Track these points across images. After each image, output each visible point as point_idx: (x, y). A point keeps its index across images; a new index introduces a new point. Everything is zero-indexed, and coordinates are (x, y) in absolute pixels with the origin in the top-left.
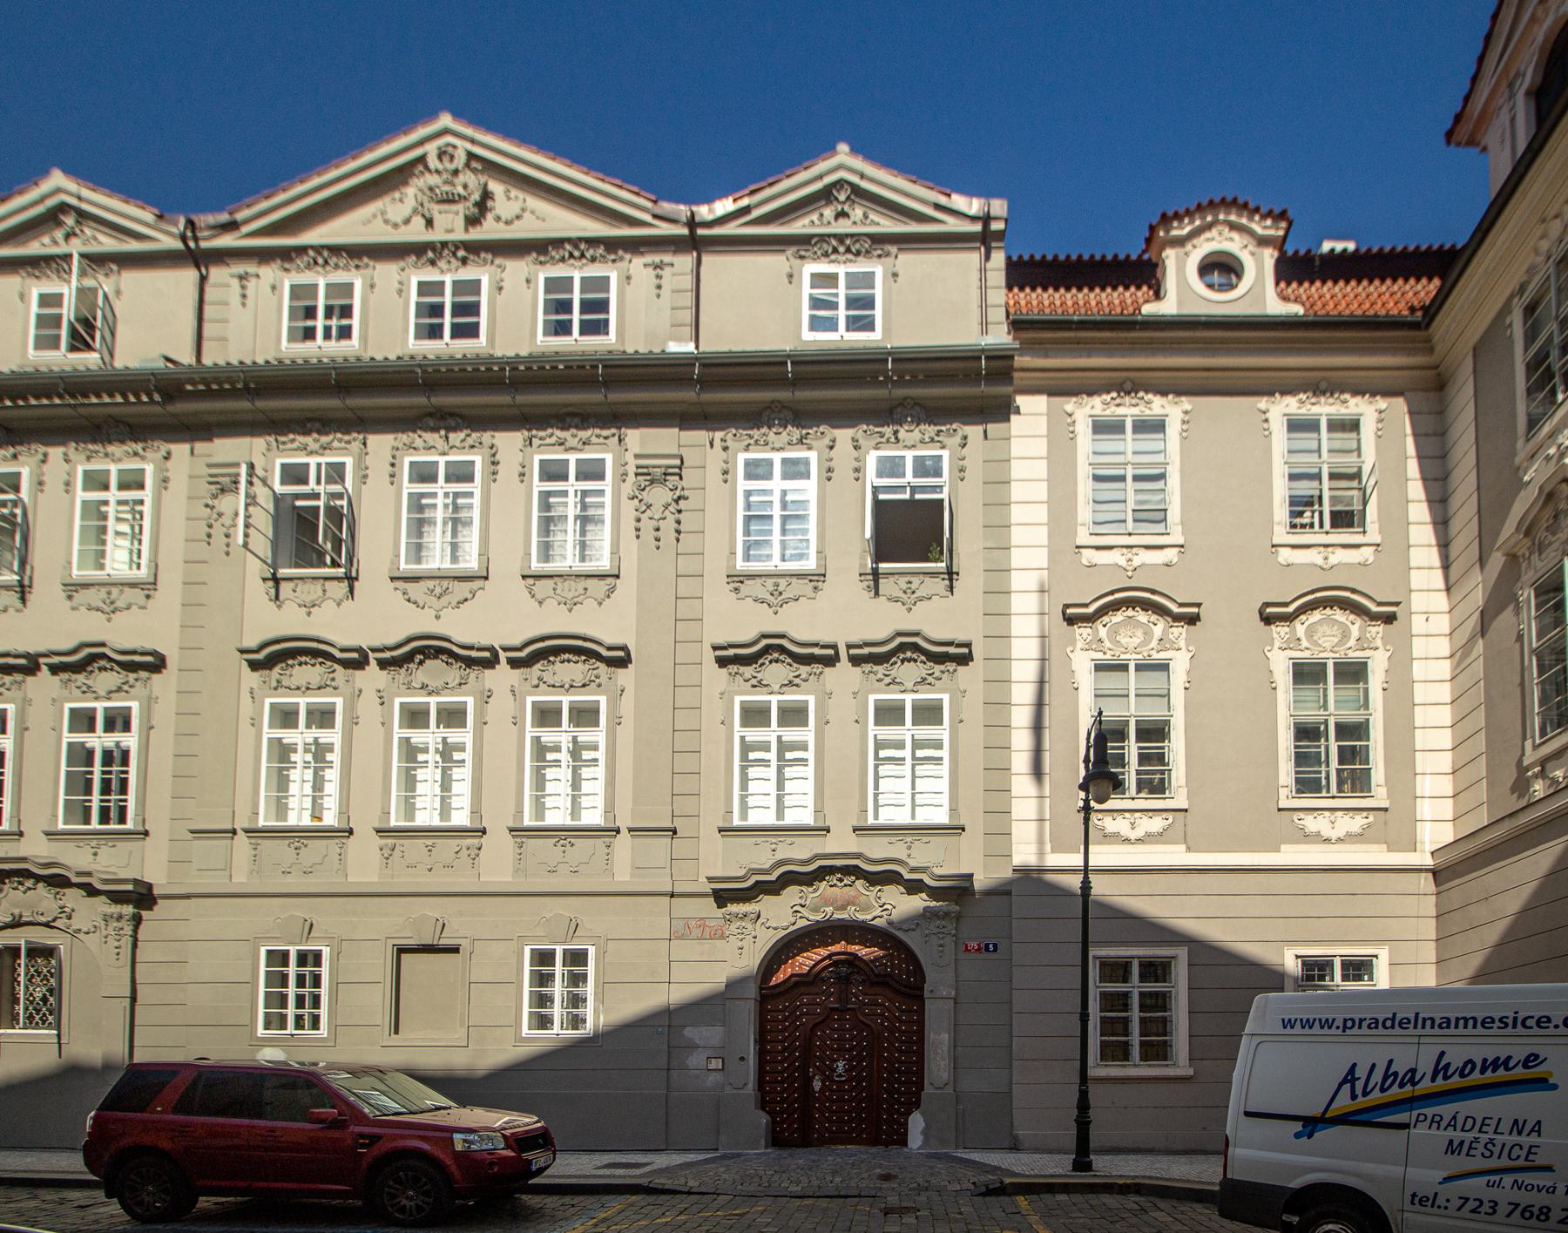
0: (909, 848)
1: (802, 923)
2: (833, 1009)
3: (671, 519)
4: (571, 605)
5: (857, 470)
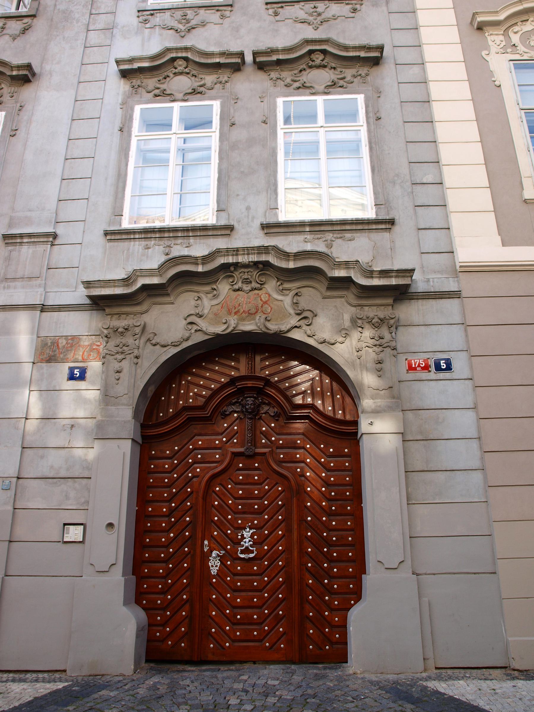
1: (198, 338)
2: (235, 455)
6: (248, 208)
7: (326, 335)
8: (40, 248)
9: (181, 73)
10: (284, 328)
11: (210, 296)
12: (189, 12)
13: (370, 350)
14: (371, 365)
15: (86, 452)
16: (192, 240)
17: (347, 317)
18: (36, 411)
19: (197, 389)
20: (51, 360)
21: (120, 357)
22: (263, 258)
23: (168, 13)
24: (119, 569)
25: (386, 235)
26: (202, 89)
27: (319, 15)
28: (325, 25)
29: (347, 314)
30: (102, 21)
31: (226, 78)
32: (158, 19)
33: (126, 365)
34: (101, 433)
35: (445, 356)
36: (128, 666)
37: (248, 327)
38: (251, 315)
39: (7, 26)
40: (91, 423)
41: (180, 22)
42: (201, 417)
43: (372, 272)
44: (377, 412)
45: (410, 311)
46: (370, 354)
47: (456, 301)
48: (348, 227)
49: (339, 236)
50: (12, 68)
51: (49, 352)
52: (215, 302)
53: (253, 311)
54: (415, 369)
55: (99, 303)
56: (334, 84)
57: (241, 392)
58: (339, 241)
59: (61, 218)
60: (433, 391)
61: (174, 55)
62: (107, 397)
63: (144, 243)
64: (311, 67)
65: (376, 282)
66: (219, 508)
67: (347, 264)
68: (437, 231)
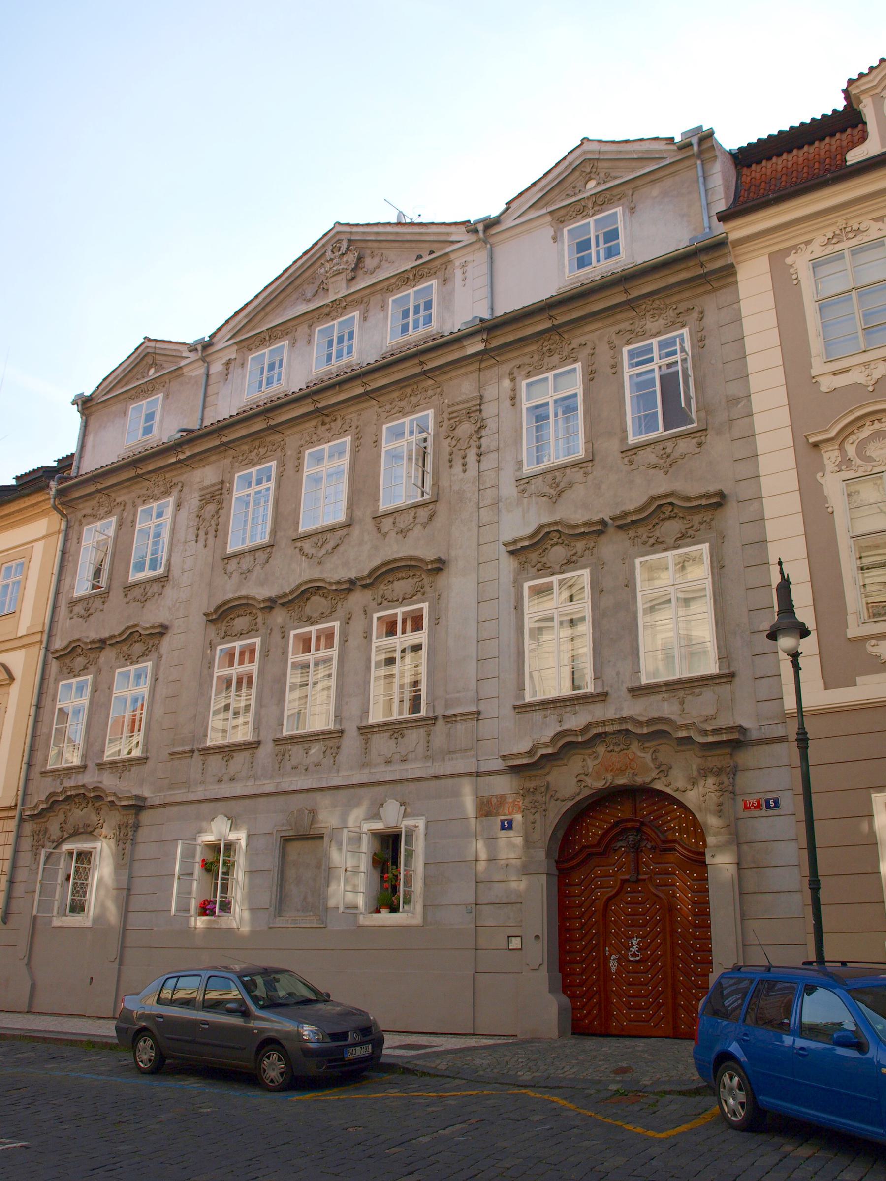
0: (682, 703)
1: (586, 793)
3: (473, 444)
4: (403, 533)
5: (613, 366)
6: (618, 673)
7: (681, 784)
8: (470, 724)
9: (557, 544)
10: (648, 780)
11: (592, 757)
12: (557, 474)
13: (713, 795)
14: (713, 807)
15: (519, 885)
16: (577, 707)
17: (694, 767)
18: (483, 855)
19: (595, 830)
20: (488, 814)
21: (533, 811)
22: (624, 727)
23: (540, 478)
24: (545, 967)
25: (728, 687)
26: (575, 558)
27: (668, 456)
28: (675, 467)
29: (695, 763)
30: (489, 496)
31: (592, 544)
32: (532, 488)
33: (537, 816)
34: (525, 871)
35: (774, 795)
36: (555, 1034)
37: (621, 781)
38: (622, 771)
39: (417, 515)
40: (517, 863)
41: (551, 487)
42: (604, 849)
43: (706, 731)
44: (720, 848)
45: (747, 757)
46: (713, 798)
47: (785, 744)
48: (696, 684)
49: (689, 692)
50: (427, 564)
51: (487, 808)
52: (597, 762)
53: (624, 768)
54: (749, 808)
55: (515, 770)
56: (683, 536)
57: (625, 830)
58: (690, 697)
59: (481, 696)
60: (765, 826)
61: (547, 530)
62: (528, 843)
63: (543, 713)
64: (662, 520)
65: (711, 739)
66: (615, 922)
67: (686, 726)
68: (770, 679)
